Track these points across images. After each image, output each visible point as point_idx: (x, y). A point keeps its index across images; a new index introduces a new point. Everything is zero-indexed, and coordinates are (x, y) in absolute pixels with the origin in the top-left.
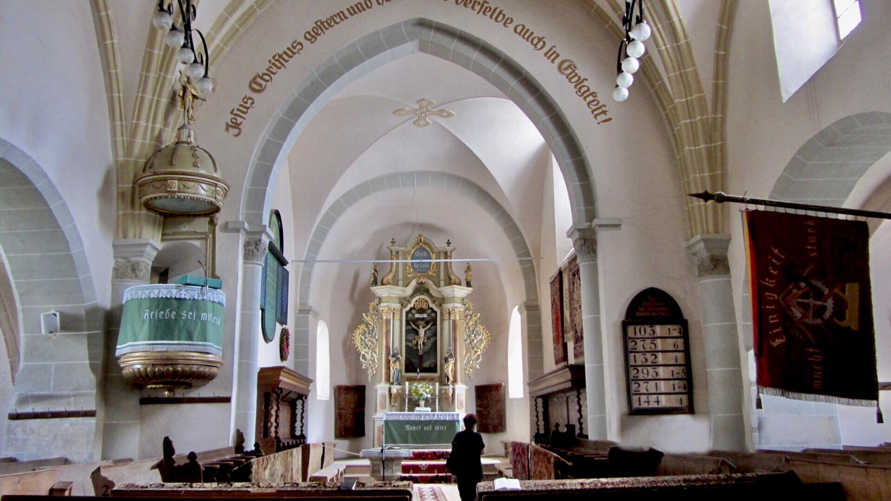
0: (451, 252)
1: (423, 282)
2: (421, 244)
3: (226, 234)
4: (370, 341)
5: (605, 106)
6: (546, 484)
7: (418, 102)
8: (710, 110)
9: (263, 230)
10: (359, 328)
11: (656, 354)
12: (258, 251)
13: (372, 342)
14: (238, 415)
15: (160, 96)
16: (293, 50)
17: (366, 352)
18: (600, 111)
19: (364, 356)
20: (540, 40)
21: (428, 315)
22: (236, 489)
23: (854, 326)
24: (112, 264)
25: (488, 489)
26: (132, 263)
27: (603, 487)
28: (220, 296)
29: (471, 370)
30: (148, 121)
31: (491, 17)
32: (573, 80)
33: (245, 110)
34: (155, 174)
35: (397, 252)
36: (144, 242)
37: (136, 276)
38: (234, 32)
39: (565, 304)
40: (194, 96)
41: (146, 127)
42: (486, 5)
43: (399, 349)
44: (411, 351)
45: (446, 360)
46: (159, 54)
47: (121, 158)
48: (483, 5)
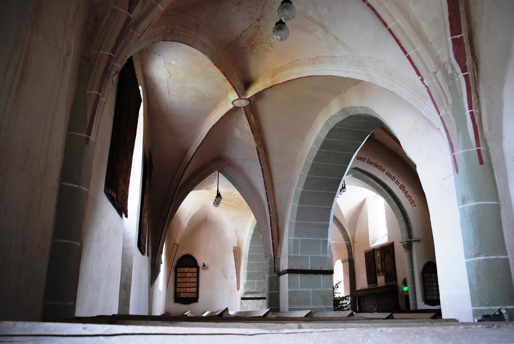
5: (414, 201)
18: (412, 202)
20: (394, 177)
31: (378, 169)
32: (404, 192)
42: (376, 164)
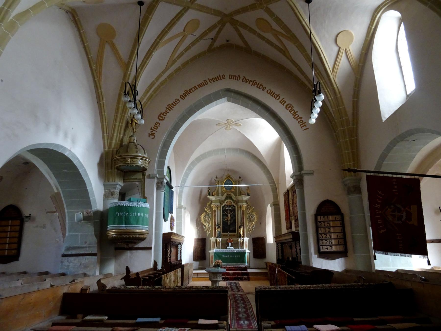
0: (241, 181)
1: (229, 194)
2: (228, 178)
3: (149, 179)
4: (208, 219)
5: (306, 123)
6: (284, 287)
7: (226, 120)
8: (351, 124)
9: (164, 177)
10: (203, 214)
11: (330, 228)
12: (162, 186)
13: (209, 220)
14: (155, 254)
15: (122, 123)
16: (176, 102)
17: (206, 224)
18: (304, 125)
19: (205, 225)
20: (278, 96)
21: (232, 208)
22: (156, 289)
23: (416, 224)
24: (103, 192)
25: (260, 289)
26: (111, 192)
27: (309, 289)
28: (147, 205)
29: (250, 231)
30: (117, 134)
31: (257, 87)
32: (292, 112)
33: (157, 128)
34: (121, 156)
35: (218, 182)
36: (117, 183)
37: (113, 197)
38: (151, 96)
39: (290, 204)
40: (136, 123)
41: (117, 136)
42: (255, 82)
43: (220, 222)
44: (225, 223)
45: (240, 228)
46: (122, 107)
47: (107, 149)
48: (253, 82)
